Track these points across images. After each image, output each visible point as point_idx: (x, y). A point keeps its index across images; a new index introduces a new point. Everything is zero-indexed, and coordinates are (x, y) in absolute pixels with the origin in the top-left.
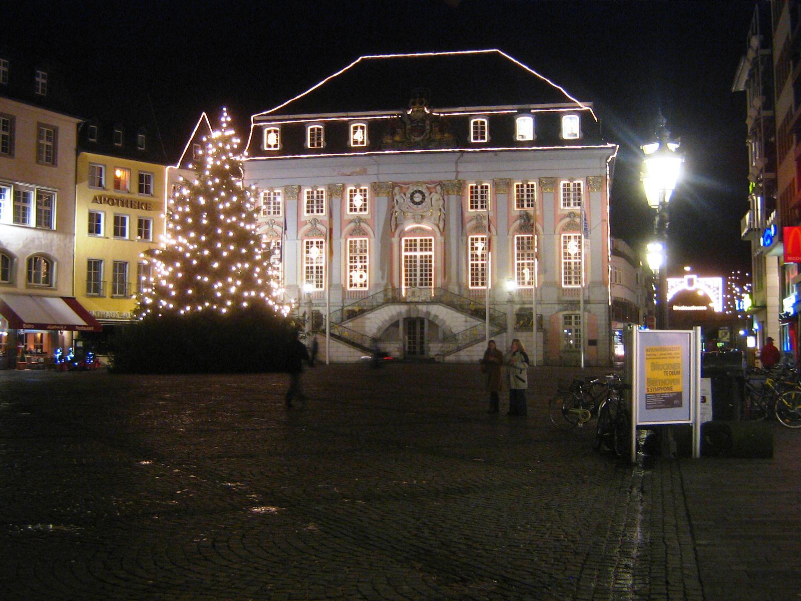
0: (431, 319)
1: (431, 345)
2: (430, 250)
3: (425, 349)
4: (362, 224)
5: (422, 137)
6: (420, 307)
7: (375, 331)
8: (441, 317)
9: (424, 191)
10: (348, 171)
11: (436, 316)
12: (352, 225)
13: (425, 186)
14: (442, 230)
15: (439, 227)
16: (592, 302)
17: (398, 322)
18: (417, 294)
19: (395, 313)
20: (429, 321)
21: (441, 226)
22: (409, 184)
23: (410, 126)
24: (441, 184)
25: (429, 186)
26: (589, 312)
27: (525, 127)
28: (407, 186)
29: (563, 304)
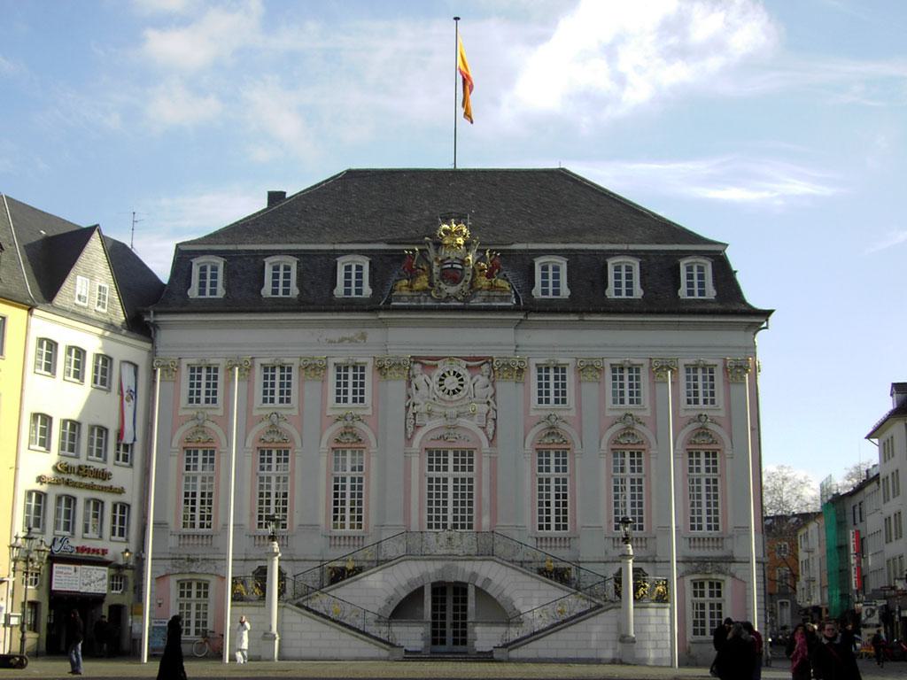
0: (479, 584)
1: (478, 629)
2: (471, 469)
3: (470, 636)
4: (358, 424)
5: (459, 286)
6: (461, 564)
7: (382, 604)
8: (496, 581)
9: (464, 372)
10: (335, 334)
11: (488, 580)
12: (340, 424)
13: (464, 363)
14: (491, 438)
15: (486, 432)
16: (737, 560)
17: (421, 590)
18: (457, 542)
19: (416, 575)
20: (476, 588)
21: (490, 431)
22: (437, 359)
23: (439, 269)
24: (488, 360)
25: (471, 364)
26: (733, 576)
27: (624, 277)
28: (435, 363)
29: (691, 562)
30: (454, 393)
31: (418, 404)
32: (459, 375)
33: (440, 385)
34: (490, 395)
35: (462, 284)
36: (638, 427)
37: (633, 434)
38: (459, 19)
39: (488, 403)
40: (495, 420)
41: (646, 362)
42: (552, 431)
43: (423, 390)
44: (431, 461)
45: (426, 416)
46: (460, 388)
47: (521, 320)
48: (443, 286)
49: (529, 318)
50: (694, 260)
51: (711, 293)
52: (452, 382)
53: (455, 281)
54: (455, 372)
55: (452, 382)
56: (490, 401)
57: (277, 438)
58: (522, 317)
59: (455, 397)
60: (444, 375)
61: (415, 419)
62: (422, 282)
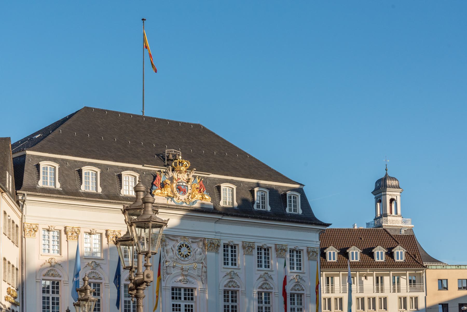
5: (185, 197)
13: (190, 240)
30: (186, 257)
31: (169, 262)
32: (188, 247)
33: (179, 252)
34: (203, 258)
35: (187, 194)
36: (270, 280)
37: (268, 284)
38: (145, 20)
39: (202, 263)
40: (206, 272)
41: (273, 246)
42: (231, 280)
43: (171, 254)
44: (173, 294)
45: (172, 268)
46: (189, 254)
47: (219, 219)
48: (178, 195)
49: (223, 218)
50: (293, 193)
51: (300, 212)
52: (184, 251)
53: (185, 193)
54: (186, 245)
55: (184, 251)
56: (204, 262)
57: (97, 276)
58: (220, 217)
59: (186, 259)
60: (181, 246)
61: (167, 270)
62: (168, 191)
